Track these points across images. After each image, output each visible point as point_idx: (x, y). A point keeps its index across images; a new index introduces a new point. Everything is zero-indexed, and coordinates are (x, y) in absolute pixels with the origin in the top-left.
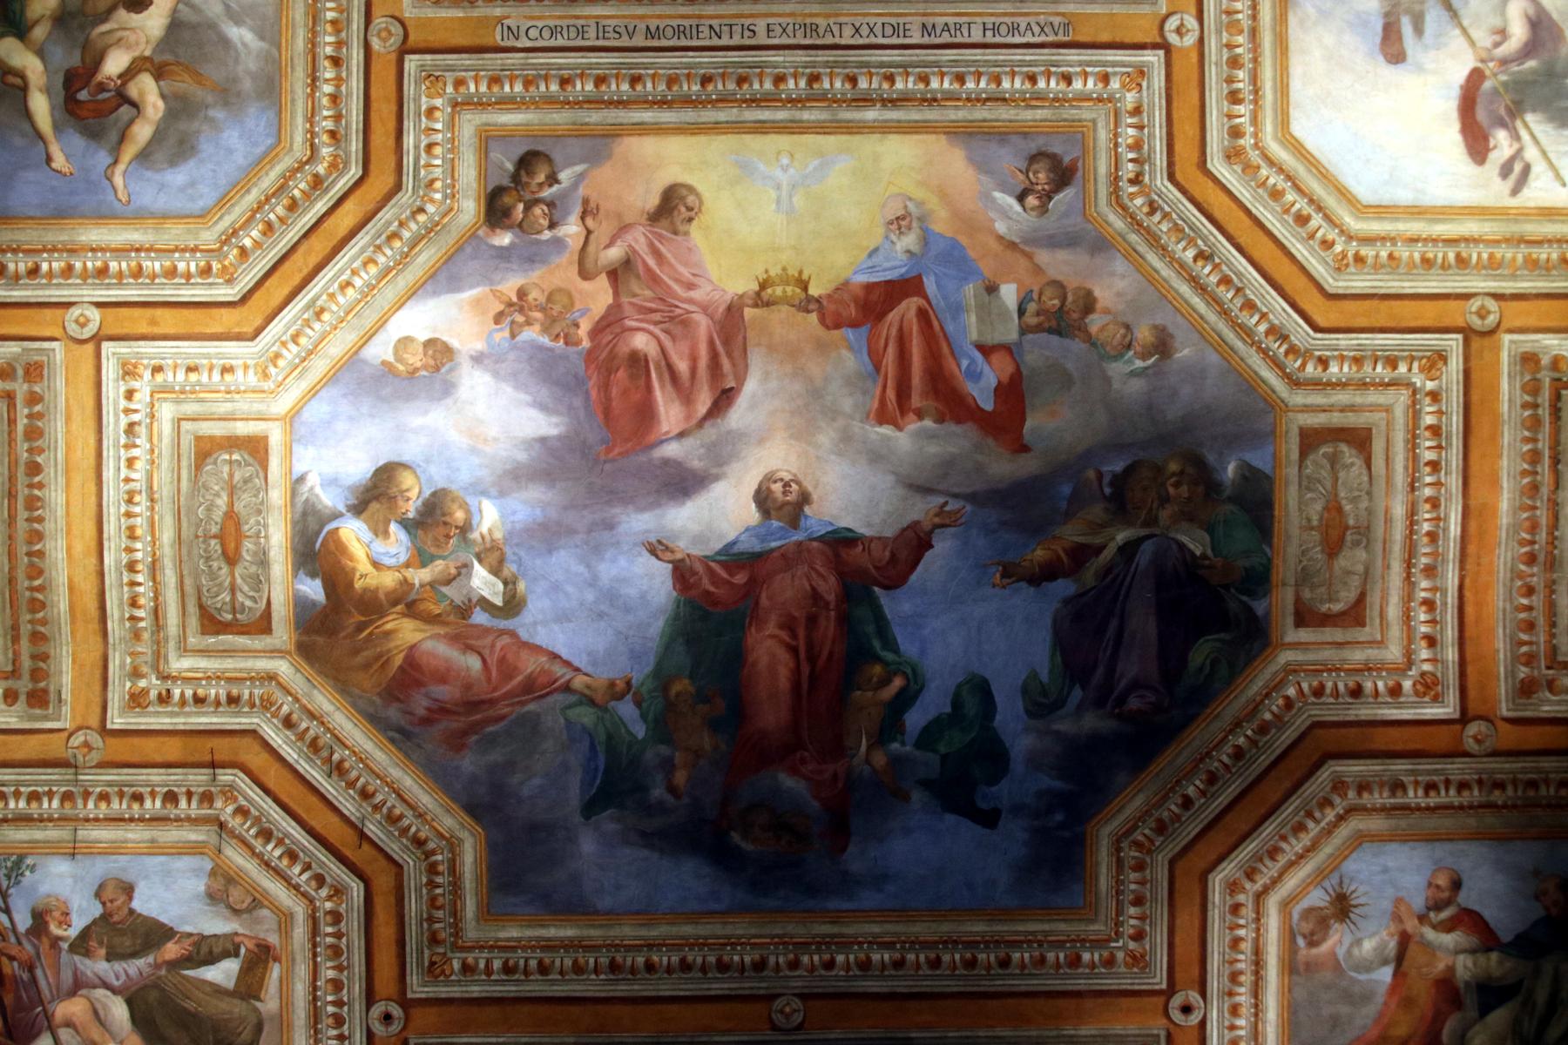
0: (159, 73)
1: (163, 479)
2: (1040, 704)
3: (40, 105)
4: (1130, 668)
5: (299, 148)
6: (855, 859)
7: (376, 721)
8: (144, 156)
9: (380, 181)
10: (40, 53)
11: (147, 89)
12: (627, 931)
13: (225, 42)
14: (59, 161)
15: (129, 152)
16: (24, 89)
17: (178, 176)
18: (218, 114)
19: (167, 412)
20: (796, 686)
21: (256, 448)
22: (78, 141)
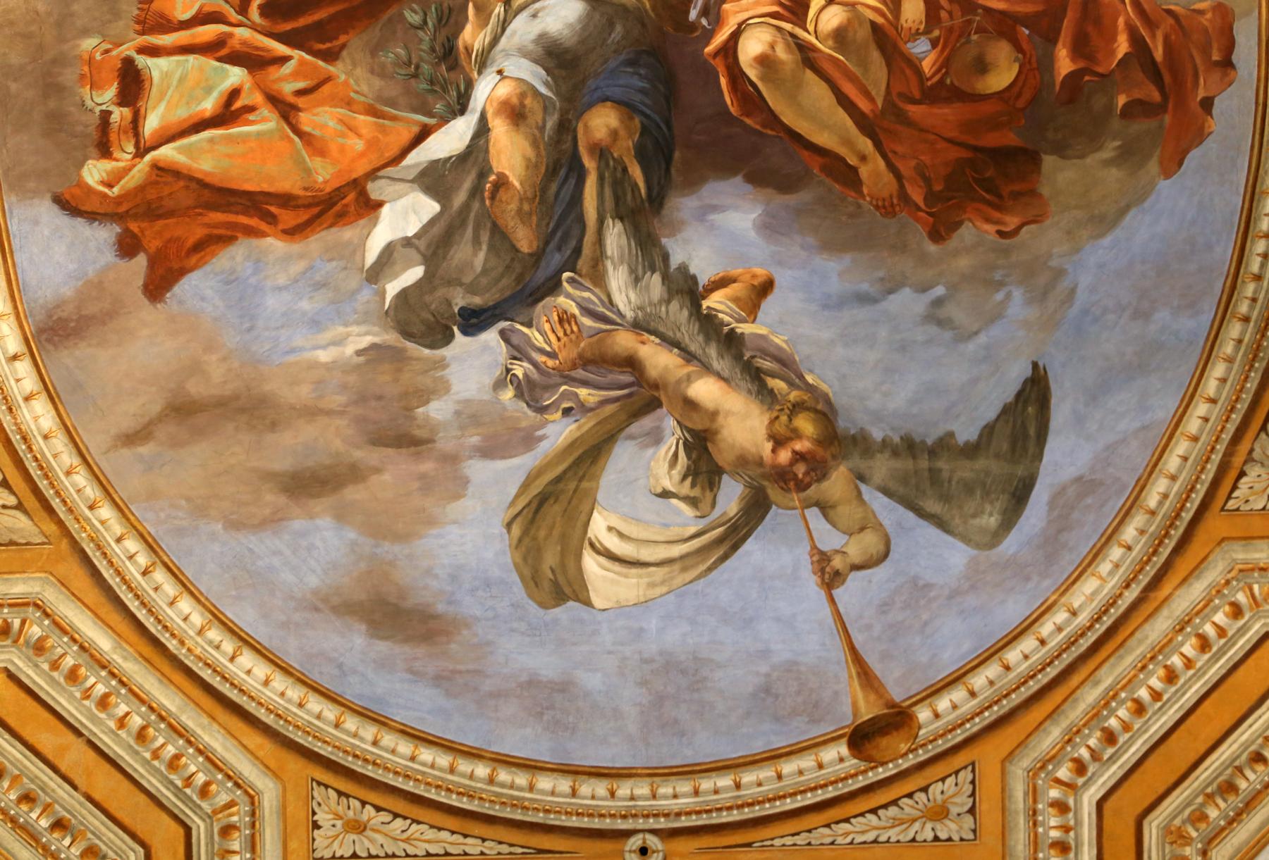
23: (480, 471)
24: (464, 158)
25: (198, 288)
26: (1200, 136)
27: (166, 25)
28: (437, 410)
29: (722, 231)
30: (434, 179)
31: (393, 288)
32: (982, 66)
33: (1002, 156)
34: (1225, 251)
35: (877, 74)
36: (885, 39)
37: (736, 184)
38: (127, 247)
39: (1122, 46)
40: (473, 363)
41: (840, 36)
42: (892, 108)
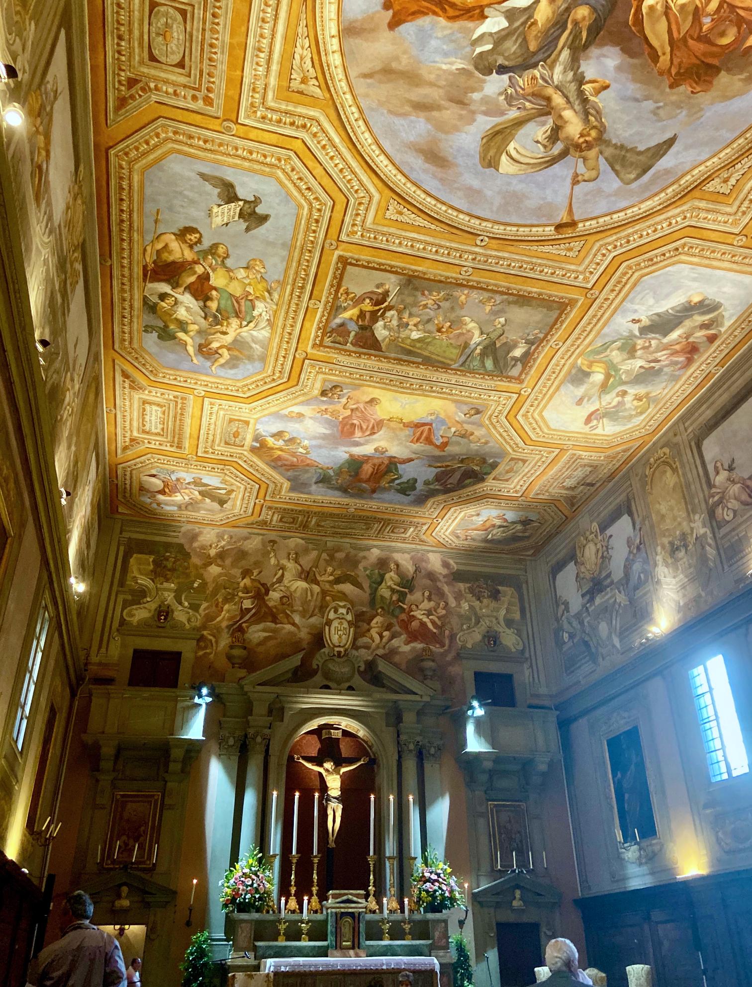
0: (229, 349)
1: (219, 423)
2: (427, 483)
3: (191, 349)
4: (450, 481)
5: (270, 372)
6: (375, 495)
7: (270, 465)
8: (222, 366)
9: (293, 382)
10: (192, 338)
11: (224, 352)
12: (319, 497)
13: (251, 347)
14: (195, 361)
15: (216, 364)
16: (186, 345)
17: (232, 372)
18: (247, 362)
19: (222, 413)
20: (372, 474)
21: (247, 423)
22: (201, 359)
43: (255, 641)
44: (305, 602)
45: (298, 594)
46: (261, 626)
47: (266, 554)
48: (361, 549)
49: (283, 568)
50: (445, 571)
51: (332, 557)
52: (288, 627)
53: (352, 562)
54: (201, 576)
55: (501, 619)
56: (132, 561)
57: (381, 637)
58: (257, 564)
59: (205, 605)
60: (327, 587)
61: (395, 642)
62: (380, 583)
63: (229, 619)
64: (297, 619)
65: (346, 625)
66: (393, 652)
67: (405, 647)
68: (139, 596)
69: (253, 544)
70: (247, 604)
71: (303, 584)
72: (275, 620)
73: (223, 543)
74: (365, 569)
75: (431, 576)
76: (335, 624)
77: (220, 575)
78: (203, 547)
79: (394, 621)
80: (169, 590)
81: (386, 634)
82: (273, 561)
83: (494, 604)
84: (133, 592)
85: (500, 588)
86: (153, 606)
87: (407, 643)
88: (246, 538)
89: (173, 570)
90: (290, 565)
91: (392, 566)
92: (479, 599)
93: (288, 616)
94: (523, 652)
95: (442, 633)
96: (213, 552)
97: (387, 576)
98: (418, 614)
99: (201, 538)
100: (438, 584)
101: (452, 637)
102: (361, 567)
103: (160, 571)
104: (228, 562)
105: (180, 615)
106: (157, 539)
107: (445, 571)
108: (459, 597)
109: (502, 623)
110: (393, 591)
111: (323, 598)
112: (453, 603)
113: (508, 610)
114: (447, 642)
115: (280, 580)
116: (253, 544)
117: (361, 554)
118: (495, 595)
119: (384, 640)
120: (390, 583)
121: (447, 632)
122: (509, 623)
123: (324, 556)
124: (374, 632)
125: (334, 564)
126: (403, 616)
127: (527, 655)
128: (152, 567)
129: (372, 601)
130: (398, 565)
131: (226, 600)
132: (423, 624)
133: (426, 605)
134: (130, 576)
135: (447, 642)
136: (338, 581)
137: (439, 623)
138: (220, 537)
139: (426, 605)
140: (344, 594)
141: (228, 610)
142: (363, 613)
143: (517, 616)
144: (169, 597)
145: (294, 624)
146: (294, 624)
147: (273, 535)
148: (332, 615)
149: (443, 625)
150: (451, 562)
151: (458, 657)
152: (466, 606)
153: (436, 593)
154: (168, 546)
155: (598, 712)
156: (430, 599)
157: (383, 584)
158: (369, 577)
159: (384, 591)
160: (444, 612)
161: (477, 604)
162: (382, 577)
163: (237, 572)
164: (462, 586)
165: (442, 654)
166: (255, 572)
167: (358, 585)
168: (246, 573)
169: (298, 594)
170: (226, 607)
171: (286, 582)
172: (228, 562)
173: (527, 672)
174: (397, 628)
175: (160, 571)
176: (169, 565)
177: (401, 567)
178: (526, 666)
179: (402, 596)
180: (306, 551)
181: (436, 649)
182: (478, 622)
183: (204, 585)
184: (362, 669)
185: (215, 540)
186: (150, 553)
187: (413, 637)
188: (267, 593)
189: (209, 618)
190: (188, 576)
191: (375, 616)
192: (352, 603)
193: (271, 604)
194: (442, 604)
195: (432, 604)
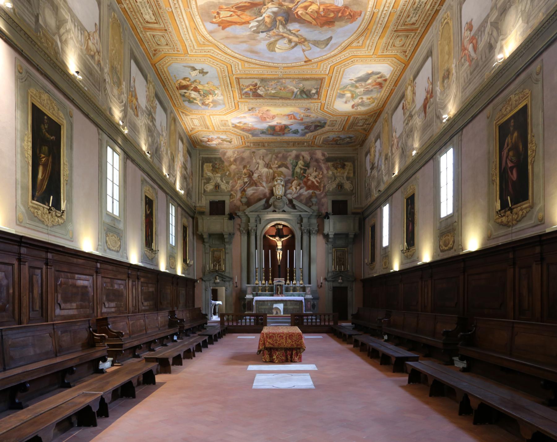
23: (263, 42)
24: (261, 20)
25: (227, 29)
26: (355, 21)
27: (222, 9)
28: (258, 38)
29: (294, 27)
30: (257, 21)
31: (252, 30)
32: (329, 15)
33: (331, 22)
34: (356, 29)
35: (316, 15)
36: (317, 12)
37: (297, 23)
38: (219, 26)
39: (348, 13)
40: (262, 35)
41: (311, 12)
42: (317, 17)
43: (250, 194)
44: (267, 177)
45: (264, 174)
46: (252, 188)
47: (251, 158)
48: (289, 152)
49: (258, 163)
50: (323, 158)
51: (277, 157)
52: (261, 188)
53: (285, 158)
54: (228, 170)
55: (345, 177)
56: (205, 166)
57: (296, 189)
58: (248, 163)
59: (231, 182)
60: (275, 170)
61: (302, 191)
62: (296, 166)
63: (240, 186)
64: (264, 184)
65: (281, 186)
66: (301, 195)
67: (305, 193)
68: (209, 180)
69: (247, 154)
70: (246, 180)
71: (266, 170)
72: (256, 185)
73: (235, 155)
74: (290, 160)
75: (317, 161)
76: (277, 186)
77: (235, 169)
78: (228, 158)
79: (301, 182)
80: (217, 177)
81: (298, 188)
82: (254, 161)
83: (342, 171)
84: (206, 179)
85: (346, 163)
86: (213, 184)
87: (306, 190)
88: (243, 152)
89: (219, 168)
90: (261, 162)
91: (301, 158)
92: (336, 169)
93: (261, 183)
94: (352, 190)
95: (320, 185)
96: (232, 159)
97: (299, 163)
98: (311, 178)
99: (227, 154)
100: (320, 164)
101: (324, 187)
102: (288, 160)
103: (215, 169)
104: (238, 163)
105: (223, 186)
106: (212, 156)
107: (323, 158)
108: (328, 169)
109: (345, 179)
110: (301, 169)
111: (274, 175)
112: (325, 172)
113: (348, 173)
114: (322, 189)
115: (257, 169)
116: (247, 154)
117: (289, 154)
118: (343, 166)
119: (298, 190)
120: (300, 166)
121: (322, 185)
122: (348, 178)
123: (274, 156)
124: (293, 188)
125: (278, 159)
126: (305, 180)
127: (354, 191)
128: (211, 168)
129: (293, 175)
130: (303, 157)
131: (239, 179)
132: (313, 182)
133: (315, 174)
134: (204, 172)
135: (322, 189)
136: (279, 167)
137: (319, 181)
138: (234, 153)
139: (315, 174)
140: (282, 172)
141: (240, 183)
142: (289, 180)
143: (352, 175)
144: (219, 180)
145: (263, 187)
146: (263, 187)
147: (253, 150)
148: (276, 183)
149: (321, 182)
150: (326, 153)
151: (326, 195)
152: (330, 173)
153: (319, 168)
154: (216, 159)
155: (370, 217)
156: (316, 171)
157: (297, 167)
158: (292, 164)
159: (298, 170)
160: (321, 176)
161: (335, 171)
162: (297, 163)
163: (241, 167)
164: (330, 164)
165: (320, 194)
166: (248, 166)
167: (287, 167)
168: (245, 167)
169: (264, 174)
170: (239, 182)
171: (259, 169)
172: (238, 163)
173: (353, 199)
174: (302, 185)
175: (215, 169)
176: (217, 166)
177: (305, 158)
178: (353, 196)
179: (305, 170)
180: (267, 155)
181: (318, 192)
182: (335, 179)
183: (230, 174)
184: (288, 203)
185: (232, 154)
186: (210, 162)
187: (309, 188)
188: (253, 175)
189: (233, 186)
190: (224, 170)
191: (293, 181)
192: (285, 176)
193: (254, 179)
194: (321, 173)
195: (317, 173)
